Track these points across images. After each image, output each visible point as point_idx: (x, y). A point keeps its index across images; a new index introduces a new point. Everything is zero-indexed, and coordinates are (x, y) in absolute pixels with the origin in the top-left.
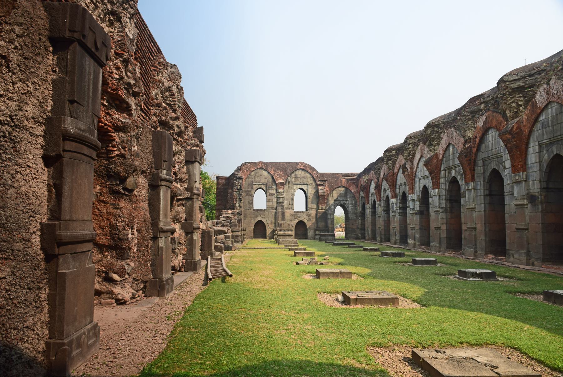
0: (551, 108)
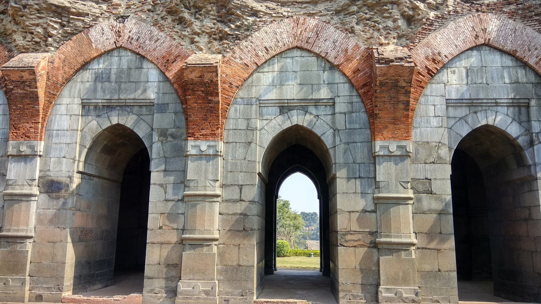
0: (120, 57)
